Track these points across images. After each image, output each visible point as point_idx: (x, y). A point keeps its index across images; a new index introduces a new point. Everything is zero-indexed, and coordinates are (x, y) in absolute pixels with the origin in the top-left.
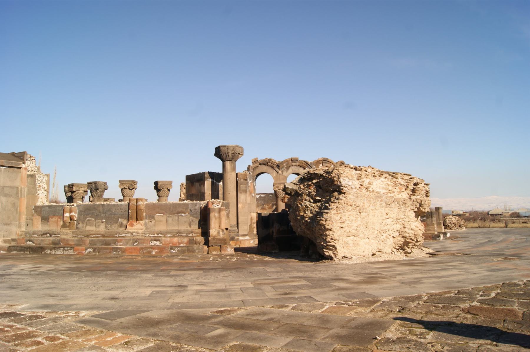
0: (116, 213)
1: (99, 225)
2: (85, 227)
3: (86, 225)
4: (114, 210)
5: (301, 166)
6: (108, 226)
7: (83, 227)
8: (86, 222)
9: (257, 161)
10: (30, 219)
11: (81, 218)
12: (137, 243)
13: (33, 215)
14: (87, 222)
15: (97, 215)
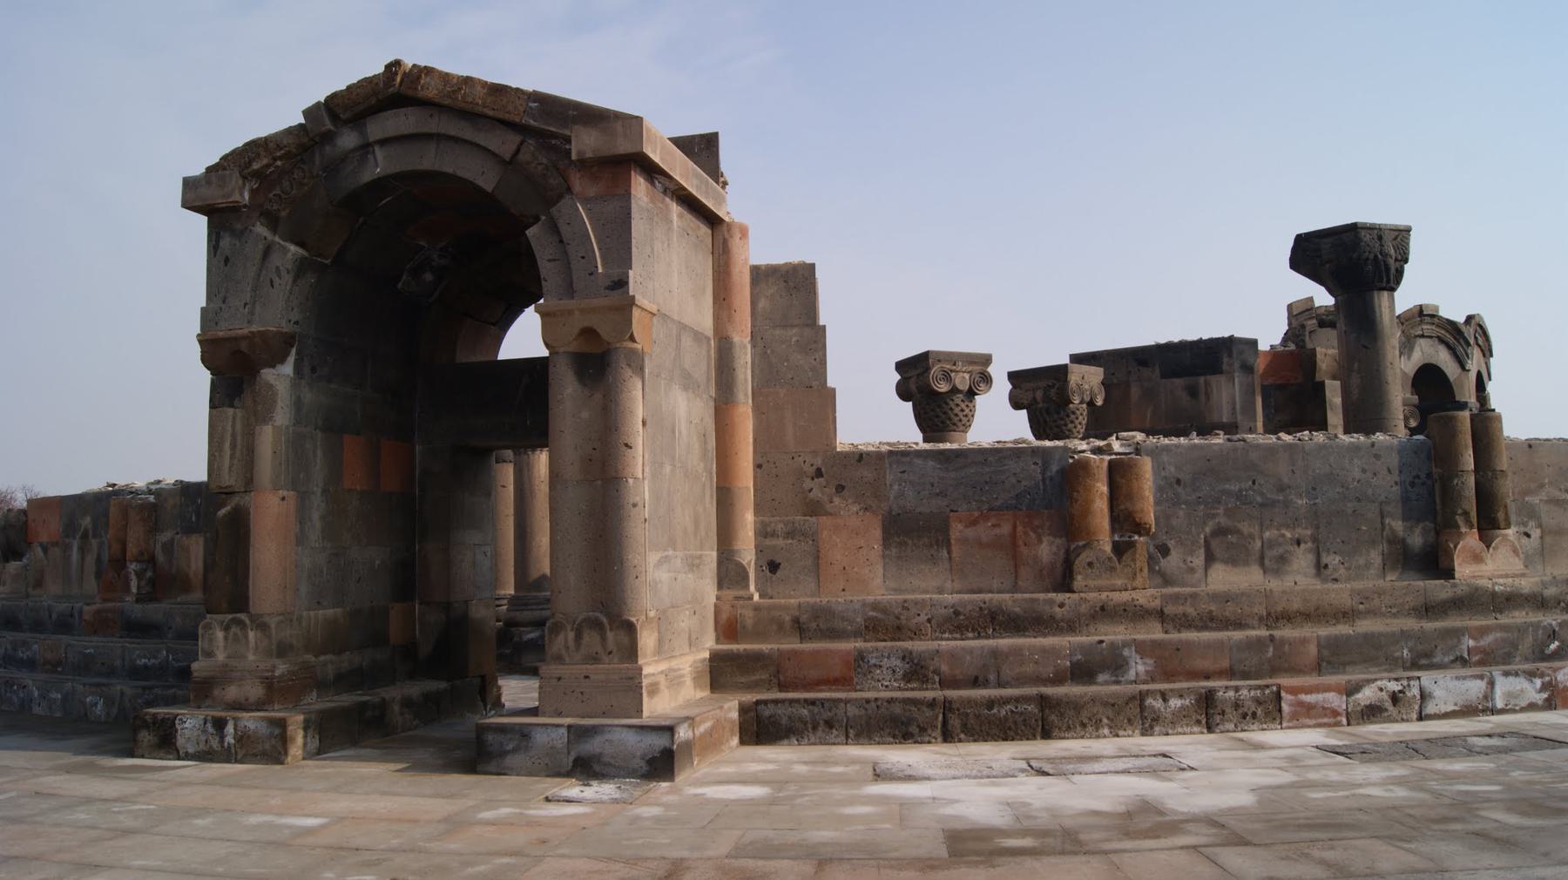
0: (1370, 492)
1: (1283, 560)
2: (1201, 571)
3: (1210, 559)
4: (1357, 474)
5: (1441, 340)
6: (1332, 560)
7: (1192, 570)
8: (1205, 541)
9: (1312, 309)
10: (790, 534)
11: (1174, 522)
12: (1557, 643)
13: (814, 509)
14: (1214, 544)
15: (1262, 505)
